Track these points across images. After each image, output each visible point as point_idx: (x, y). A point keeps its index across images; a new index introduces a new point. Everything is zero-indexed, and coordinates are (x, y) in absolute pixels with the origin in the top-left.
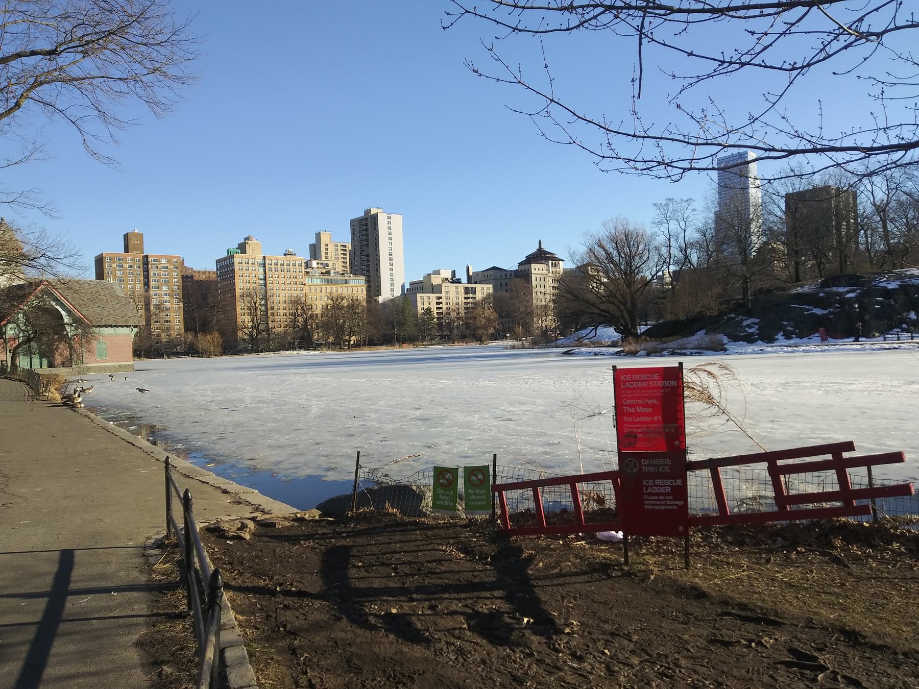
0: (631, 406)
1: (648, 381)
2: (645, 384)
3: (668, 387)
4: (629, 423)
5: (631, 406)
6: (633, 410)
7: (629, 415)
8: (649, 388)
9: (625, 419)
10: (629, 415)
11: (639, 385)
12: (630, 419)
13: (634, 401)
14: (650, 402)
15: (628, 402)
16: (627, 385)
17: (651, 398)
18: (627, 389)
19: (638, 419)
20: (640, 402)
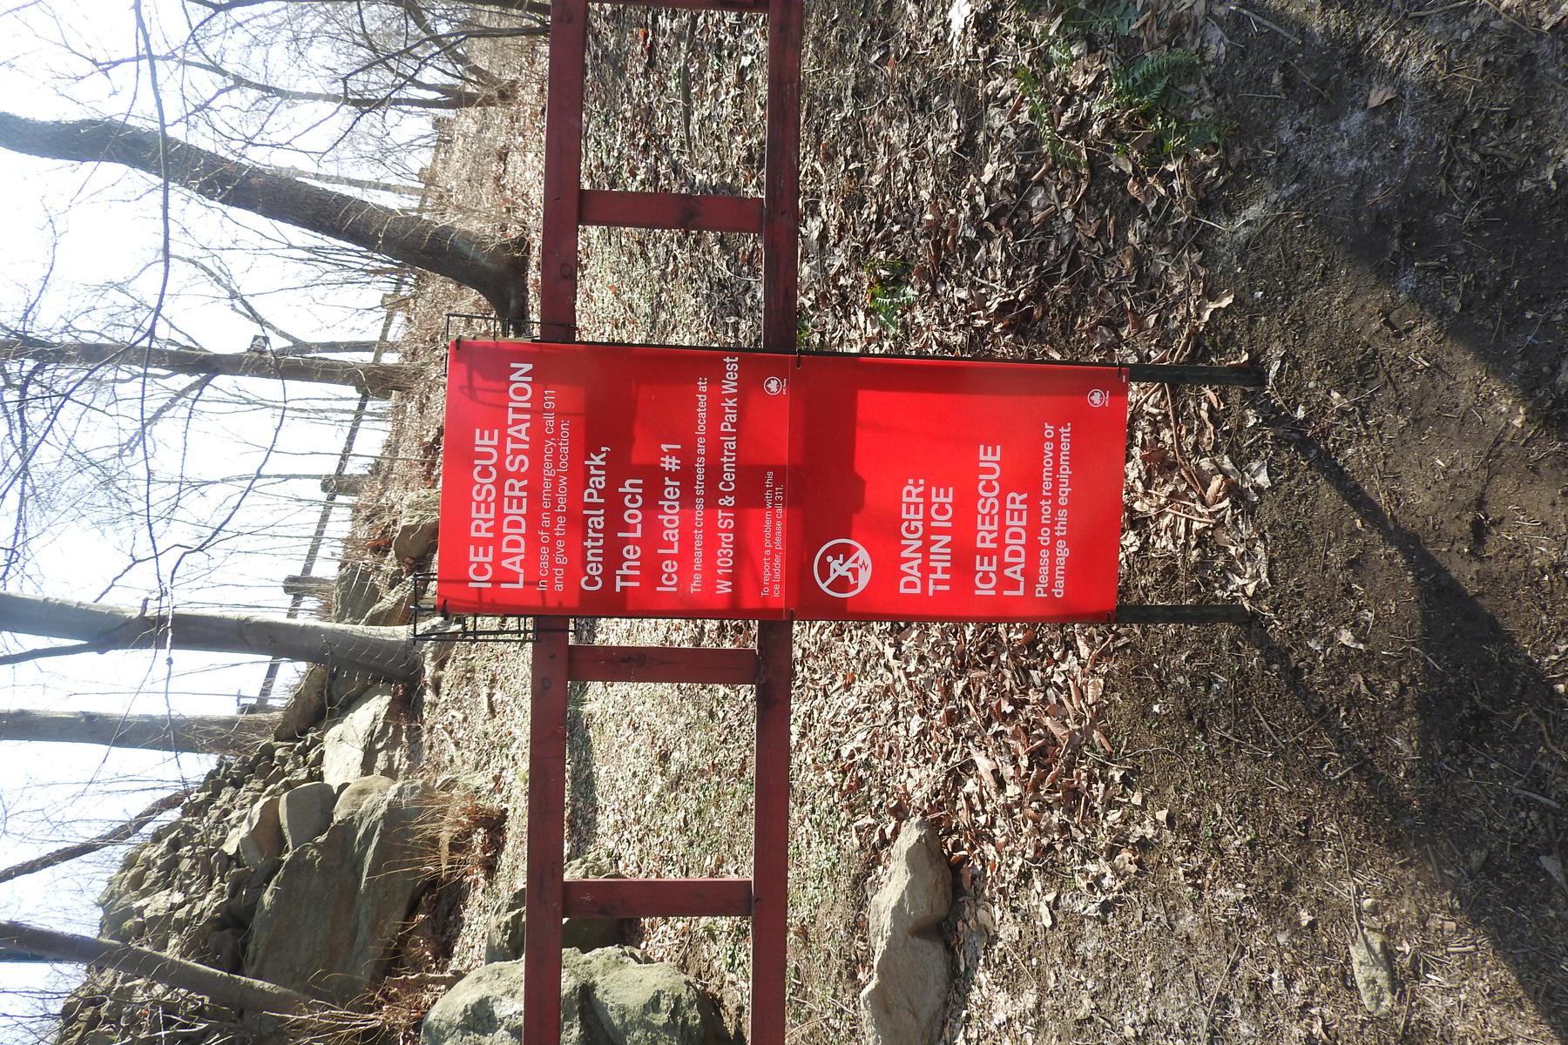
0: (612, 559)
1: (503, 474)
2: (515, 488)
3: (537, 399)
4: (685, 572)
5: (612, 559)
6: (632, 554)
7: (651, 569)
8: (533, 479)
9: (668, 586)
10: (651, 569)
11: (516, 513)
12: (669, 567)
13: (593, 546)
14: (599, 481)
15: (595, 569)
16: (514, 564)
17: (581, 477)
18: (530, 562)
19: (671, 534)
20: (597, 520)
